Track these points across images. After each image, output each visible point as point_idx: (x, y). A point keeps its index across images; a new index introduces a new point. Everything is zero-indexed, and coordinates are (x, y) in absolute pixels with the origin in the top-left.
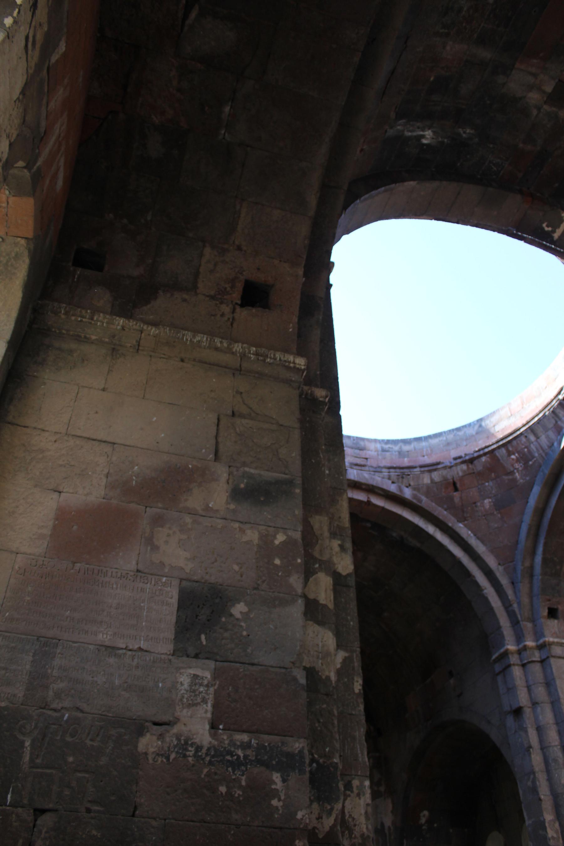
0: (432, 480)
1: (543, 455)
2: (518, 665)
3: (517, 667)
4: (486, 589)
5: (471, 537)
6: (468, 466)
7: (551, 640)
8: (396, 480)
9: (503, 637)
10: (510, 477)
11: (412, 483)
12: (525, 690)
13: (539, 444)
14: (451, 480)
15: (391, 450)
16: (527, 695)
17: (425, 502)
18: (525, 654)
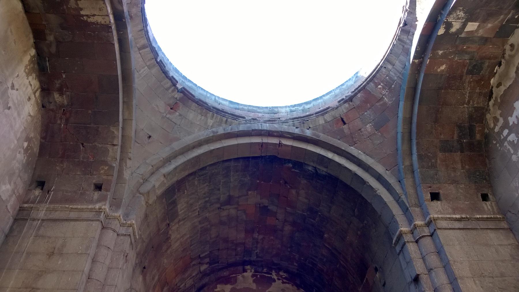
0: (325, 120)
1: (401, 76)
2: (412, 242)
3: (411, 244)
4: (378, 190)
5: (361, 154)
6: (349, 104)
7: (436, 216)
8: (299, 126)
9: (396, 222)
10: (381, 103)
11: (311, 126)
12: (421, 260)
13: (396, 69)
14: (339, 117)
15: (297, 110)
16: (423, 265)
17: (323, 137)
18: (416, 232)
